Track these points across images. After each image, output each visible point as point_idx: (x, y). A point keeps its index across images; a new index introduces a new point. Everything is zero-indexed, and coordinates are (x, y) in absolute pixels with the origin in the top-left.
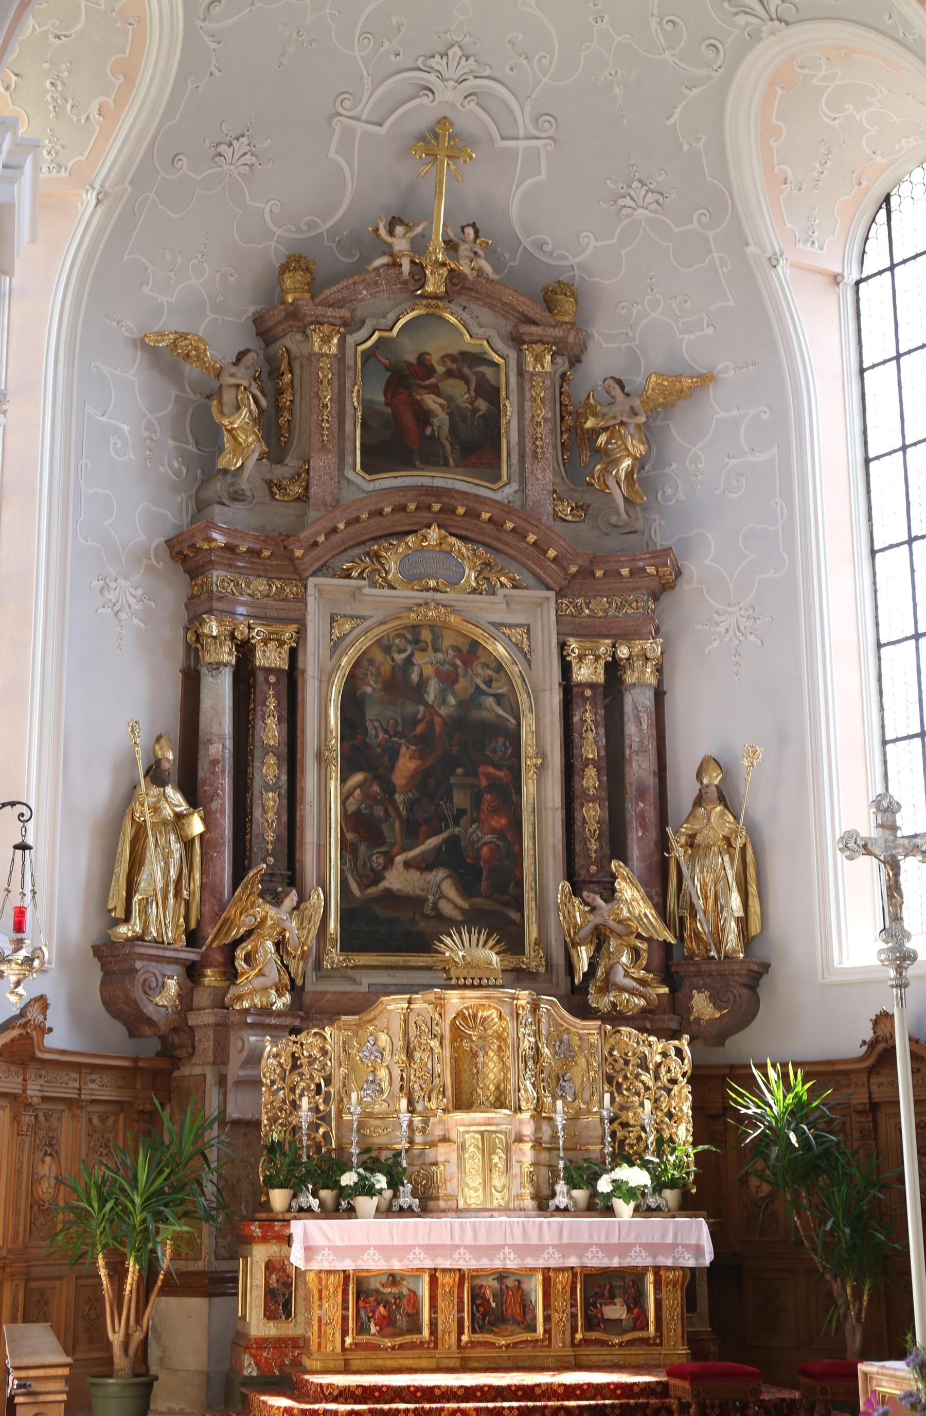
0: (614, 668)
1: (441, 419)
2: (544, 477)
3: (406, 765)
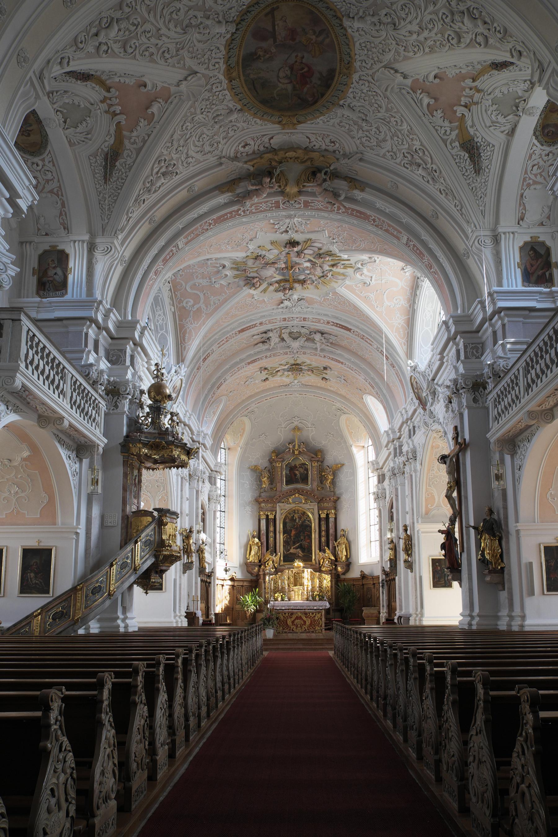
0: (327, 515)
1: (298, 475)
2: (315, 484)
3: (293, 532)
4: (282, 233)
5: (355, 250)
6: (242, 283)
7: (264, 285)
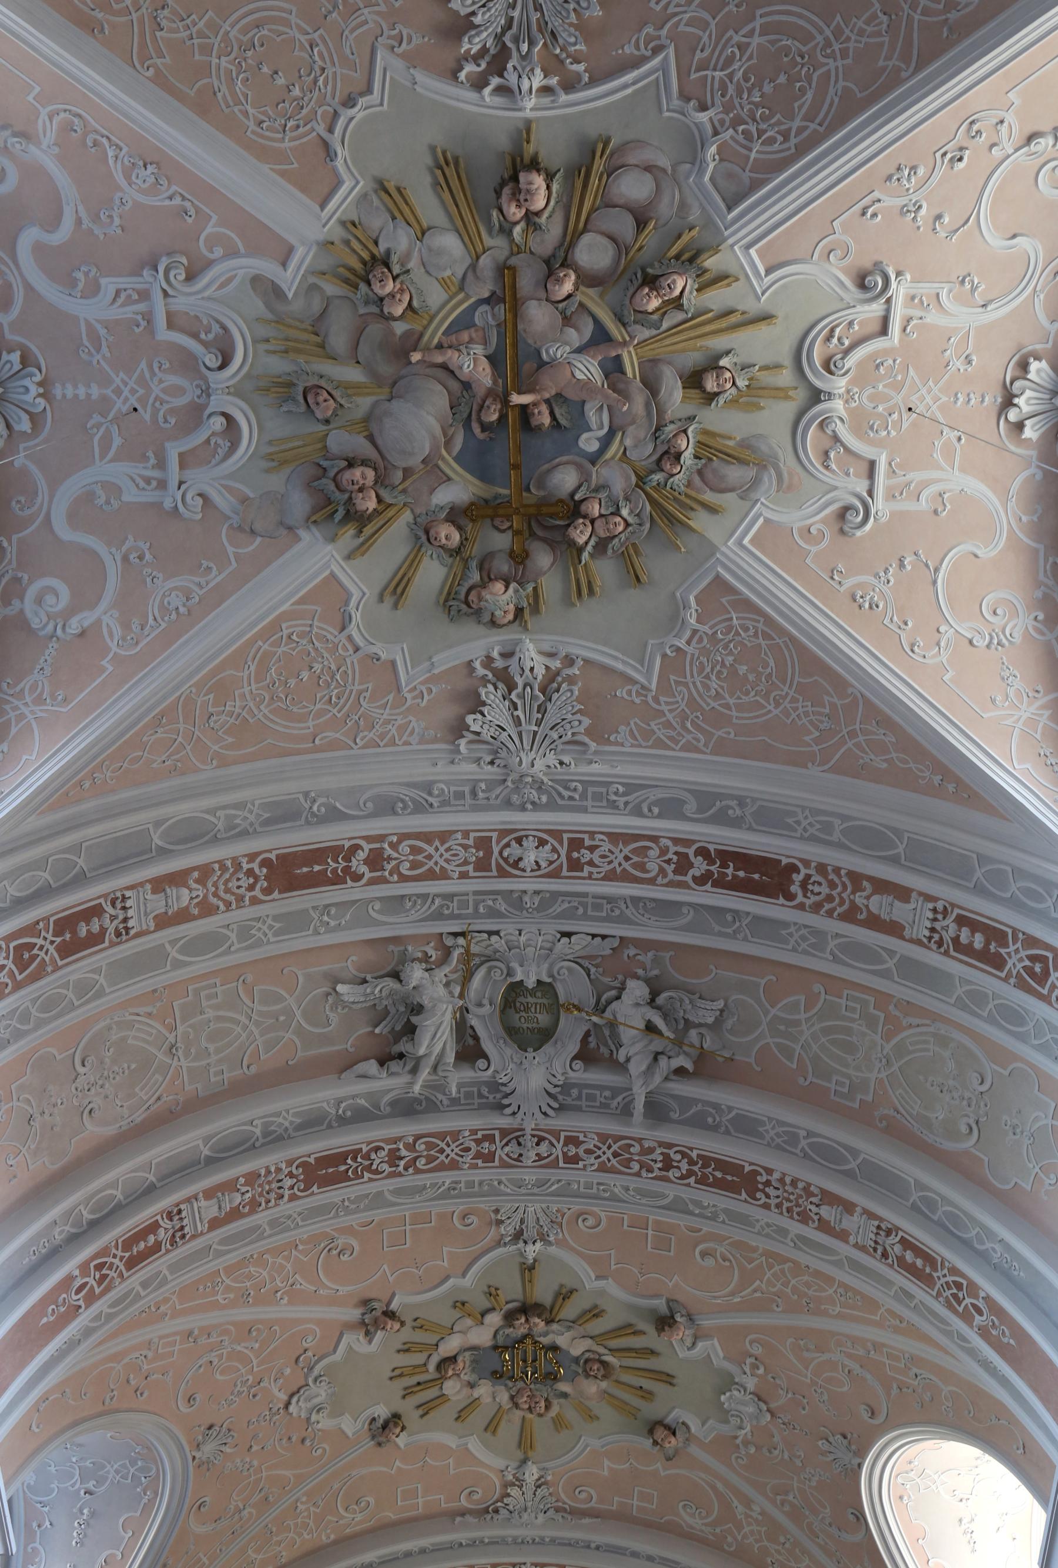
4: (479, 84)
5: (802, 150)
6: (300, 503)
7: (394, 540)
